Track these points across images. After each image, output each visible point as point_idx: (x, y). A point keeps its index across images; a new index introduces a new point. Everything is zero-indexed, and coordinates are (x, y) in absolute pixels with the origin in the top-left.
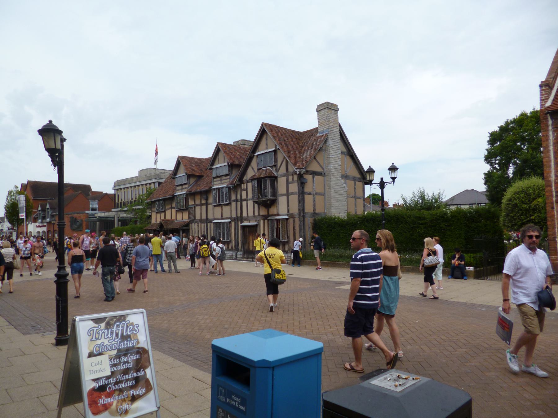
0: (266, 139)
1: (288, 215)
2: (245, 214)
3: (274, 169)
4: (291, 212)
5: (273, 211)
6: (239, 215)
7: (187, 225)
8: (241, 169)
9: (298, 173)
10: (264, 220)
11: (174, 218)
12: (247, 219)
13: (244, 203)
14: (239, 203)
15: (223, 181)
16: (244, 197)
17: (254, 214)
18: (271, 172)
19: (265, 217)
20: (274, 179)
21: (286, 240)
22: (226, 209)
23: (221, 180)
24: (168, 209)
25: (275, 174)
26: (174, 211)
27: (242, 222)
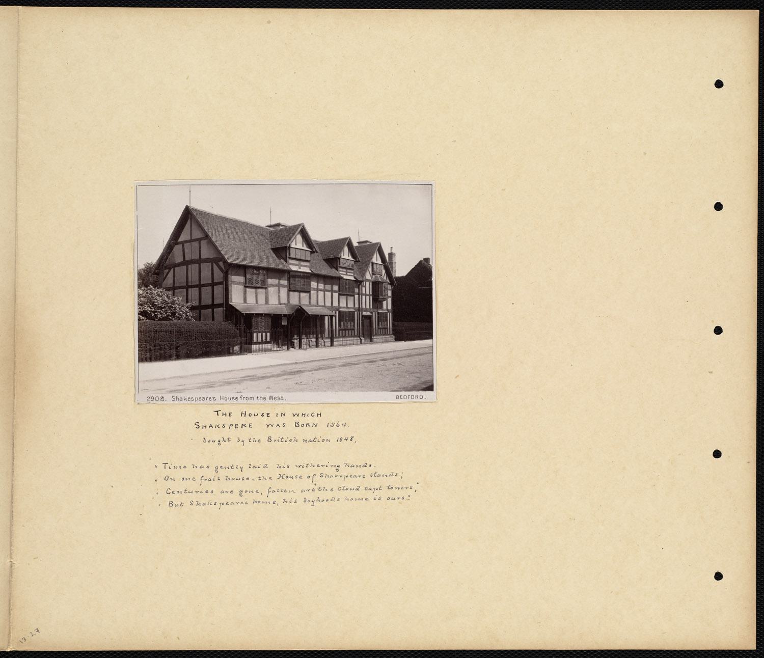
2: (364, 306)
12: (366, 310)
13: (364, 297)
15: (348, 274)
16: (364, 292)
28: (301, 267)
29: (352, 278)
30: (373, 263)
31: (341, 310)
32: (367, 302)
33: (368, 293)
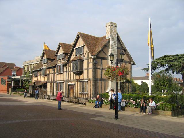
0: (80, 41)
2: (69, 79)
3: (83, 56)
4: (89, 78)
5: (81, 77)
6: (67, 79)
7: (46, 83)
8: (68, 56)
9: (92, 58)
10: (77, 82)
11: (41, 80)
12: (70, 81)
13: (69, 73)
16: (70, 70)
18: (81, 57)
19: (78, 80)
20: (82, 61)
21: (86, 93)
22: (62, 76)
25: (83, 58)
26: (41, 76)
27: (68, 83)
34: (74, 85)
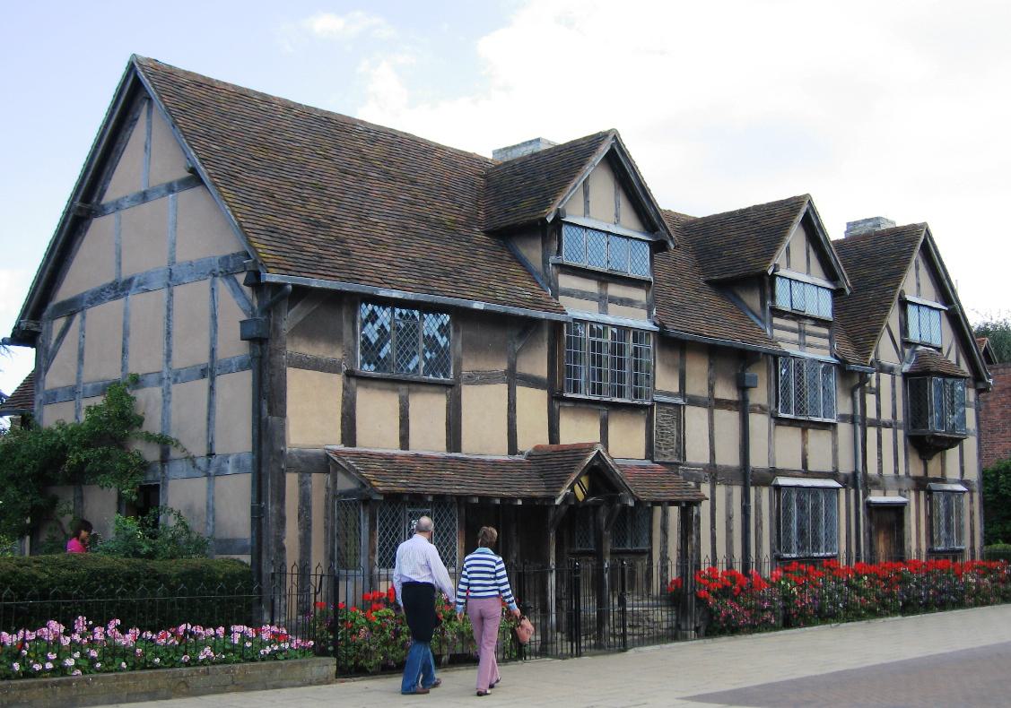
1: (963, 482)
2: (872, 469)
5: (934, 468)
10: (917, 491)
13: (872, 433)
14: (859, 429)
15: (809, 339)
16: (871, 413)
17: (896, 471)
23: (802, 333)
24: (488, 379)
28: (611, 306)
29: (825, 356)
30: (904, 304)
31: (782, 481)
32: (887, 454)
33: (886, 416)
34: (899, 510)
